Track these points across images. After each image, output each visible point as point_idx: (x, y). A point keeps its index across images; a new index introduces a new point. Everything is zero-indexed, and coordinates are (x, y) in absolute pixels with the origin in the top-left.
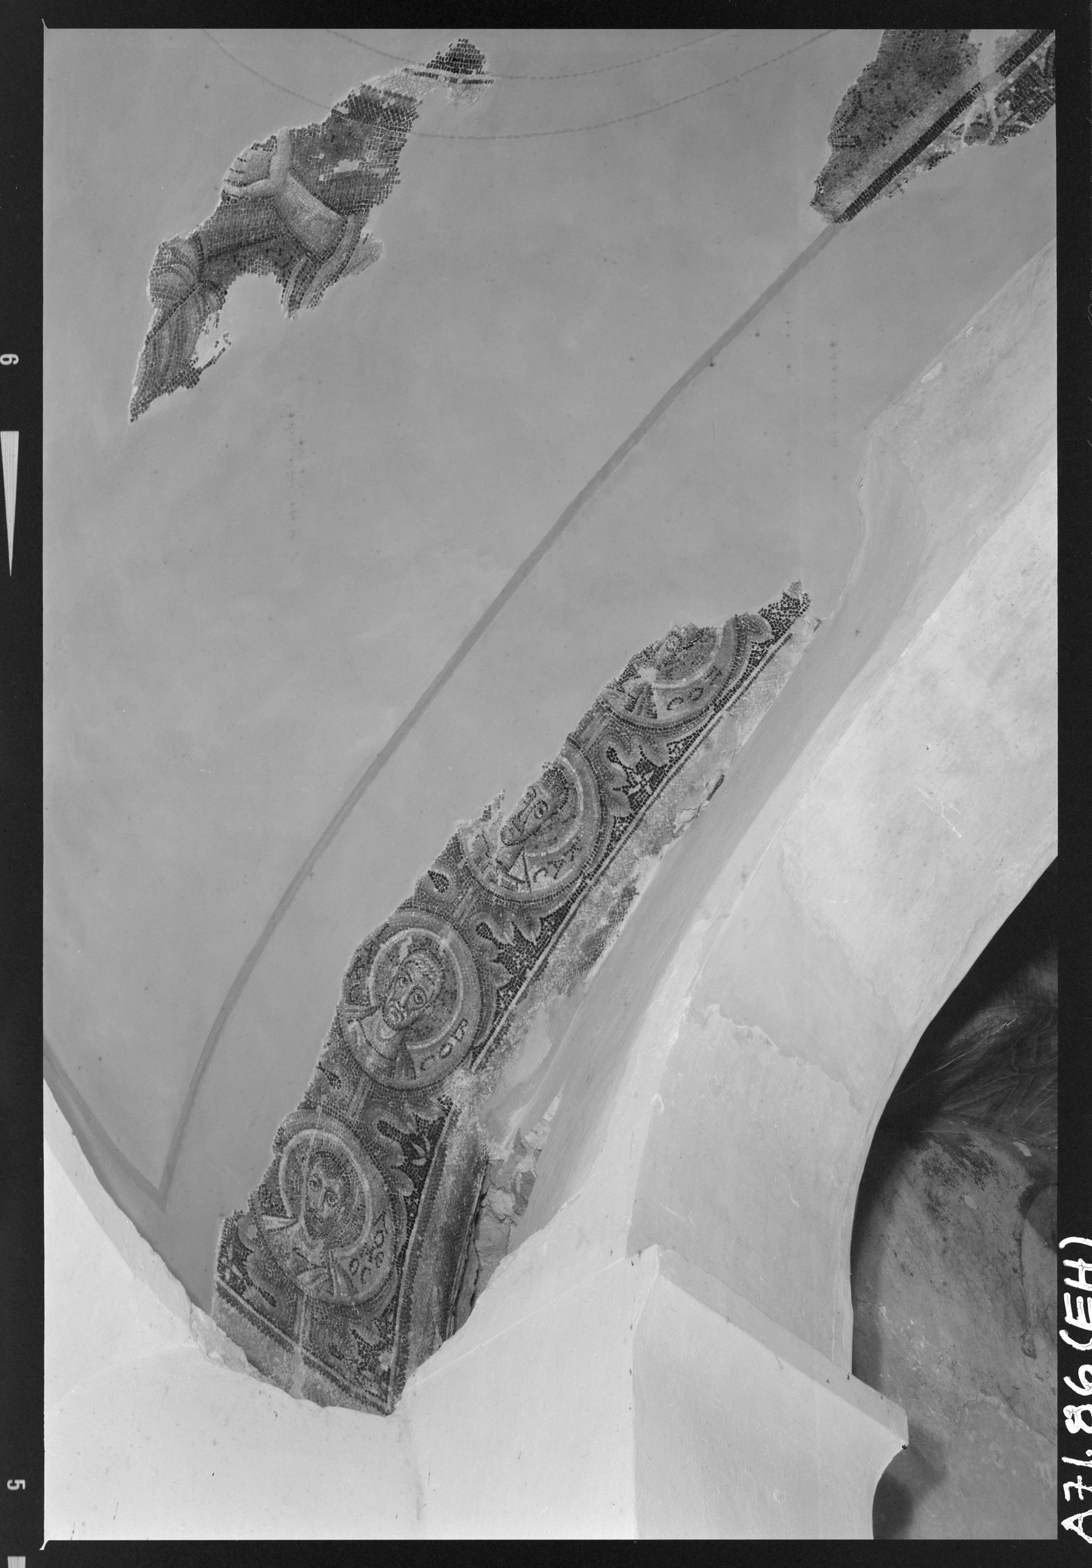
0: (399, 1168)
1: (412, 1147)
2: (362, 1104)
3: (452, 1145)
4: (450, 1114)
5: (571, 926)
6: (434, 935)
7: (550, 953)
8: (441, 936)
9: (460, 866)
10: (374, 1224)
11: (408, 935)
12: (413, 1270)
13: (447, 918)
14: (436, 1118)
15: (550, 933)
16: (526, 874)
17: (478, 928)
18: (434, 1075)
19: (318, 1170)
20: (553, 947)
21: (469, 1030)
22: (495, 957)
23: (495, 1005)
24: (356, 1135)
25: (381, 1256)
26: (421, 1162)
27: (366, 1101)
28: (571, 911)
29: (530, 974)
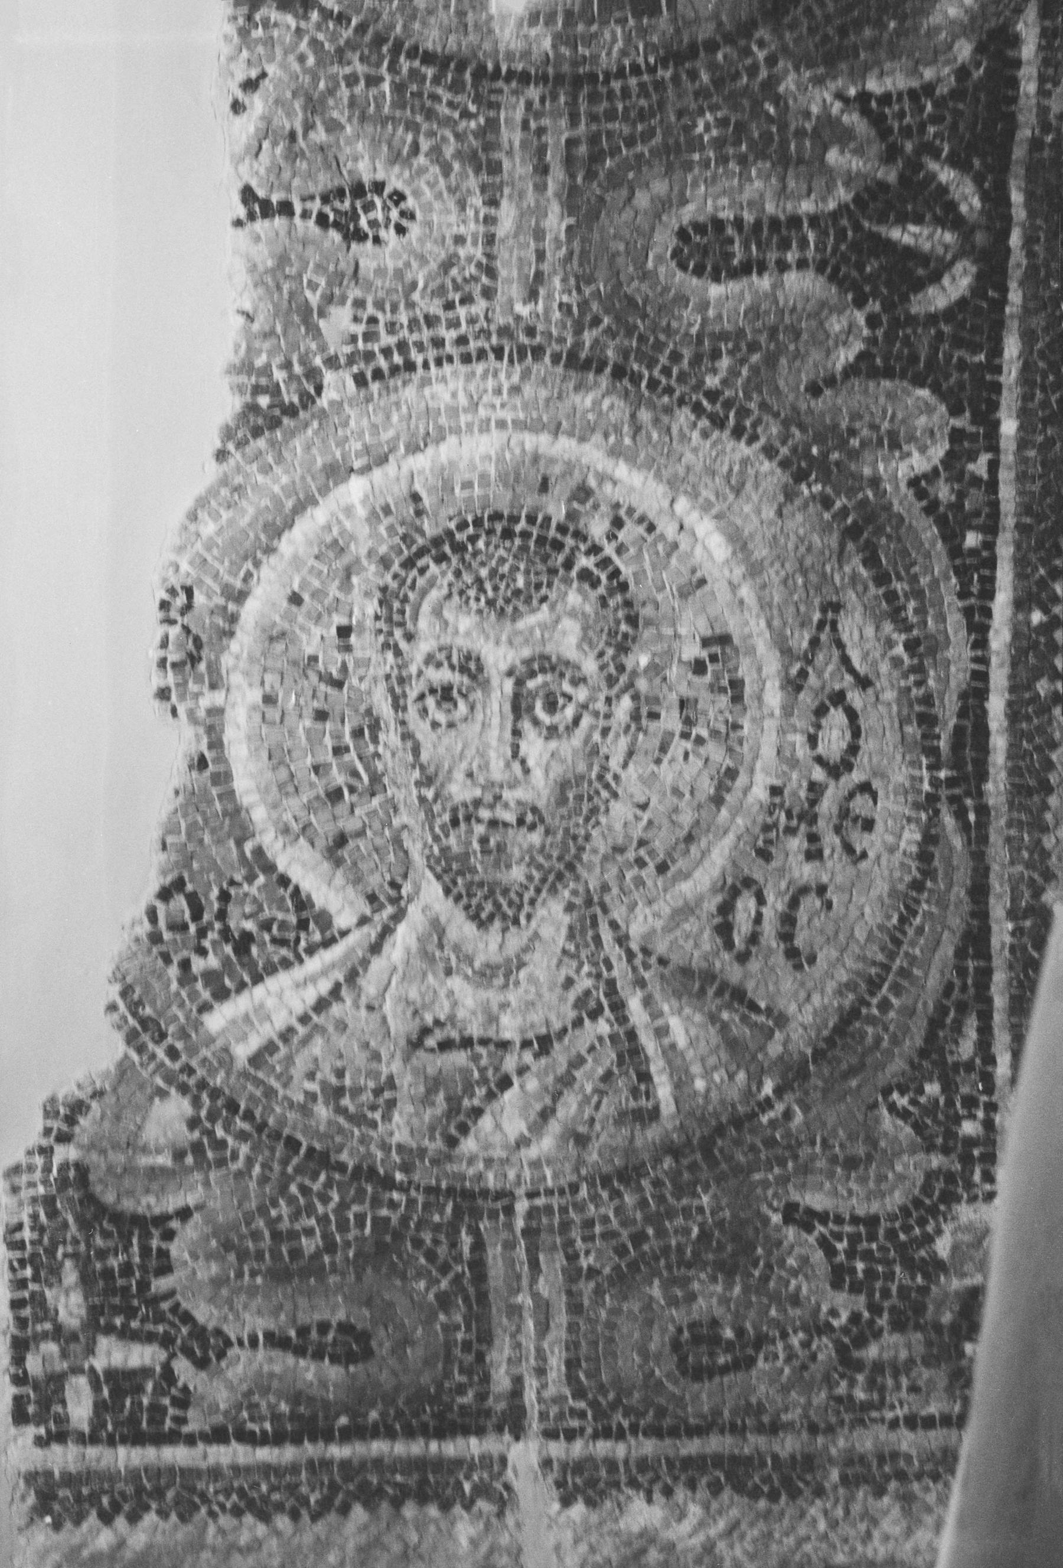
0: (851, 371)
2: (556, 222)
10: (794, 685)
12: (1032, 784)
14: (964, 50)
24: (579, 364)
25: (860, 805)
26: (958, 283)
27: (571, 200)
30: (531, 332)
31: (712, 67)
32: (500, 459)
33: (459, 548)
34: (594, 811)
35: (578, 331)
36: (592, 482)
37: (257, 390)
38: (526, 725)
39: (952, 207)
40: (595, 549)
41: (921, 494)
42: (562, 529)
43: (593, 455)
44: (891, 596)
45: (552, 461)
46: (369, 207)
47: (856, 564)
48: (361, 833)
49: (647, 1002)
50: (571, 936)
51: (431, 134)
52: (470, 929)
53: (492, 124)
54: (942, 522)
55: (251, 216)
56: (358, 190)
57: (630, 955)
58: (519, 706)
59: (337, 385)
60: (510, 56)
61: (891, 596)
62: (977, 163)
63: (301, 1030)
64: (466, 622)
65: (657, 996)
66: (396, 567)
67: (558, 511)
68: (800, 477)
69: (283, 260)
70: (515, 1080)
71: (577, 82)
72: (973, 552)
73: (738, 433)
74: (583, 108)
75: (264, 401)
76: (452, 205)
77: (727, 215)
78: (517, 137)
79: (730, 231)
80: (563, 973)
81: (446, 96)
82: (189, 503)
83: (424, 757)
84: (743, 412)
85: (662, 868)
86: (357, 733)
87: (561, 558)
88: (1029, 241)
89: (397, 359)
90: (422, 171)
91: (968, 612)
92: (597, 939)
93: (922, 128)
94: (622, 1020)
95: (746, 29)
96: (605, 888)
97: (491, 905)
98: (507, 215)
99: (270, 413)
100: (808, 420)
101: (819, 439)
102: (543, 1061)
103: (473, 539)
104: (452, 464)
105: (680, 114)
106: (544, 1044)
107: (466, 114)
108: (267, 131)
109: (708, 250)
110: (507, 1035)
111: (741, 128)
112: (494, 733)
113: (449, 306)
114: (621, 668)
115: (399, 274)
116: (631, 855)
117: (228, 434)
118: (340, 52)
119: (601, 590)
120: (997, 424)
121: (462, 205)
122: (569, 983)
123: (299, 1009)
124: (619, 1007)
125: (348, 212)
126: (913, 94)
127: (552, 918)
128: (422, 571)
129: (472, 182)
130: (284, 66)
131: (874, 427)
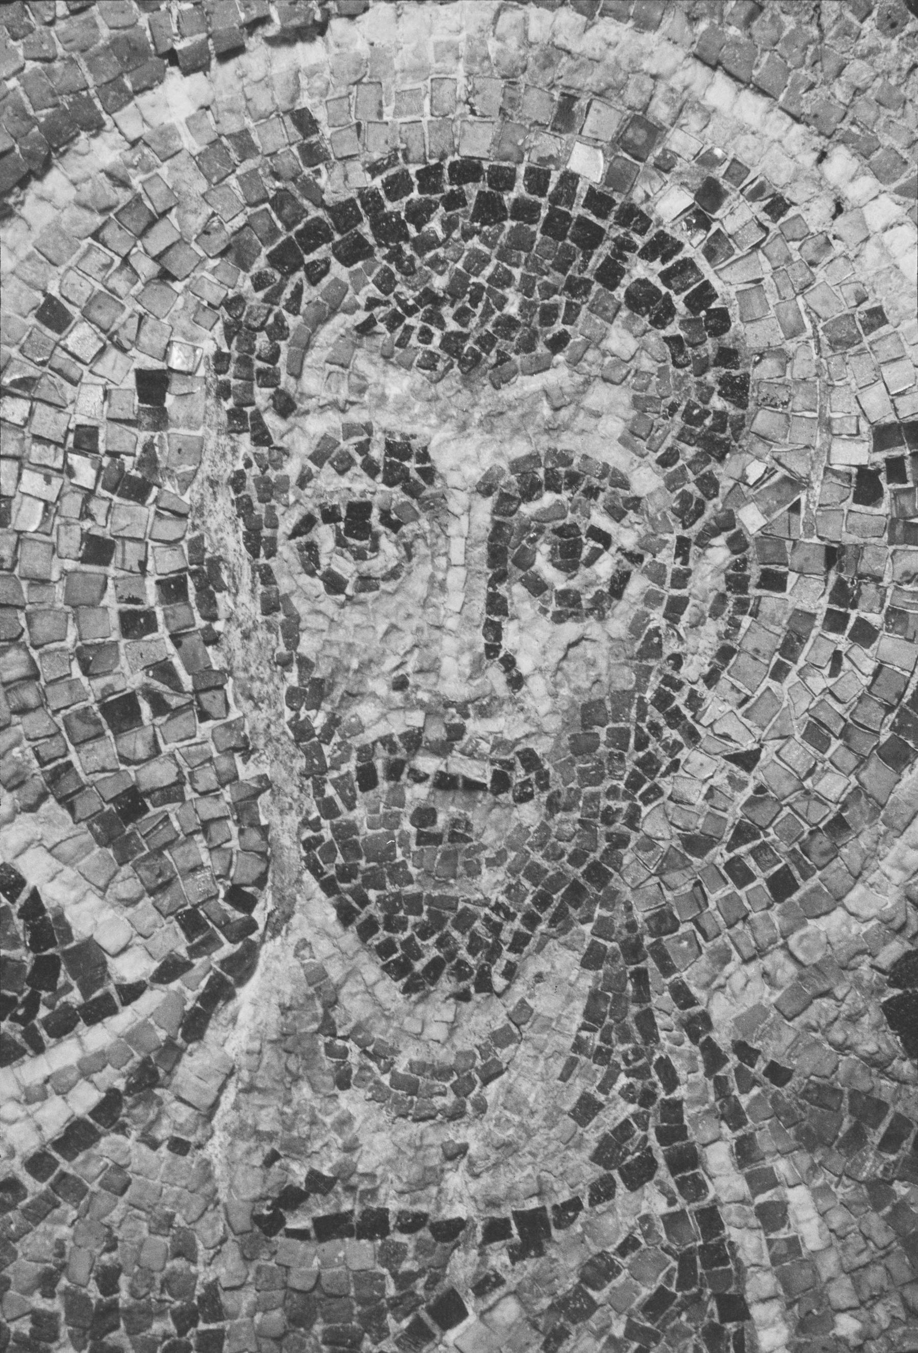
19: (363, 387)
33: (391, 231)
34: (649, 765)
36: (661, 112)
38: (516, 592)
40: (662, 247)
42: (598, 202)
48: (171, 793)
49: (745, 1152)
50: (592, 1017)
52: (390, 992)
57: (713, 1057)
58: (503, 553)
63: (35, 1187)
64: (398, 384)
65: (765, 1143)
66: (260, 263)
67: (588, 164)
70: (470, 1304)
80: (578, 1086)
83: (307, 645)
85: (782, 886)
86: (172, 589)
87: (595, 262)
92: (646, 1021)
94: (694, 1187)
96: (663, 921)
97: (430, 945)
102: (530, 1265)
103: (419, 214)
106: (532, 1231)
110: (460, 1211)
112: (455, 601)
114: (709, 484)
116: (720, 855)
119: (673, 329)
122: (587, 1109)
123: (27, 1142)
124: (686, 1160)
127: (557, 979)
128: (316, 274)
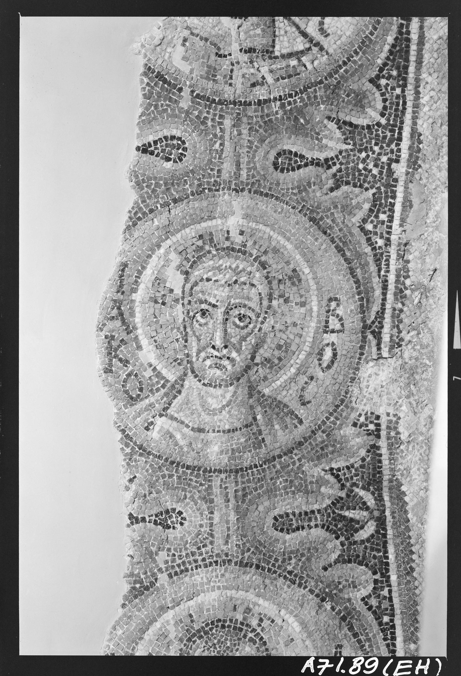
1: (344, 518)
2: (233, 517)
3: (408, 470)
4: (383, 433)
5: (426, 56)
6: (209, 223)
7: (415, 118)
8: (224, 216)
9: (185, 104)
11: (167, 253)
13: (215, 187)
14: (363, 453)
15: (398, 91)
16: (304, 34)
17: (276, 165)
18: (330, 398)
20: (416, 106)
21: (347, 309)
22: (331, 183)
23: (368, 250)
24: (243, 564)
26: (371, 528)
27: (237, 509)
28: (414, 37)
29: (400, 169)
30: (227, 555)
31: (280, 463)
32: (219, 600)
33: (206, 633)
35: (243, 554)
36: (251, 606)
37: (135, 582)
39: (364, 503)
40: (254, 630)
41: (366, 604)
42: (242, 624)
43: (251, 596)
44: (359, 641)
45: (237, 599)
46: (171, 517)
47: (346, 630)
51: (190, 492)
53: (210, 487)
54: (374, 613)
55: (132, 523)
56: (167, 512)
59: (163, 578)
60: (214, 464)
61: (359, 641)
62: (371, 488)
66: (185, 642)
67: (240, 617)
68: (323, 600)
69: (143, 536)
71: (237, 472)
72: (387, 624)
73: (300, 585)
74: (239, 479)
75: (138, 586)
76: (198, 514)
77: (290, 511)
78: (218, 490)
79: (291, 517)
81: (194, 479)
82: (113, 623)
84: (301, 578)
87: (242, 635)
88: (393, 513)
89: (182, 568)
90: (188, 504)
91: (388, 645)
93: (352, 478)
95: (290, 451)
98: (217, 517)
99: (141, 589)
100: (324, 579)
101: (328, 586)
103: (211, 629)
104: (203, 603)
105: (271, 479)
107: (201, 485)
108: (136, 495)
109: (283, 524)
111: (291, 481)
113: (199, 548)
115: (182, 538)
117: (126, 598)
118: (160, 468)
119: (257, 645)
120: (389, 577)
121: (202, 514)
125: (164, 519)
126: (348, 468)
128: (194, 642)
129: (205, 506)
130: (142, 474)
131: (347, 581)
